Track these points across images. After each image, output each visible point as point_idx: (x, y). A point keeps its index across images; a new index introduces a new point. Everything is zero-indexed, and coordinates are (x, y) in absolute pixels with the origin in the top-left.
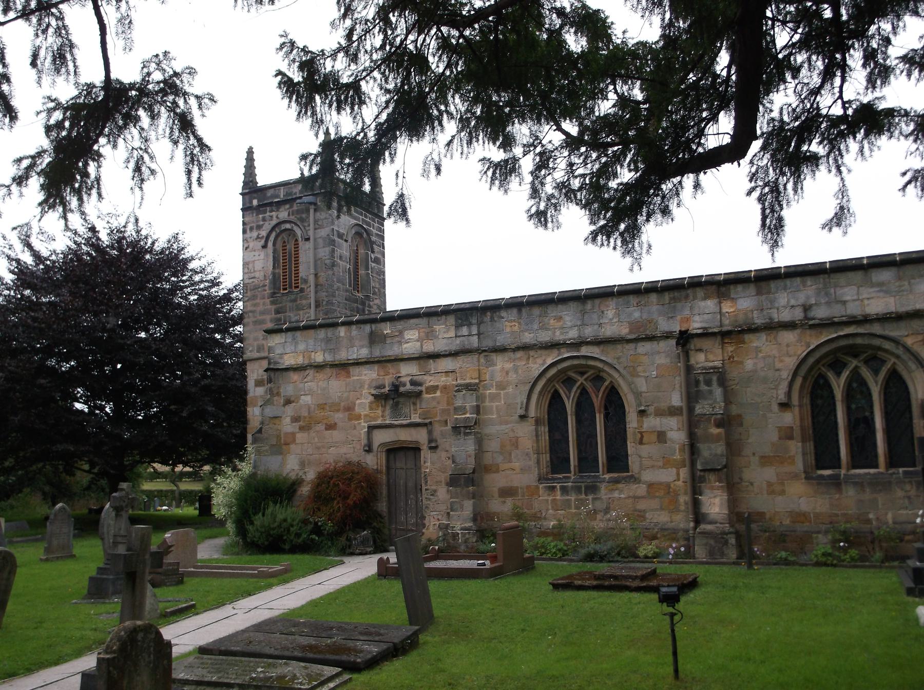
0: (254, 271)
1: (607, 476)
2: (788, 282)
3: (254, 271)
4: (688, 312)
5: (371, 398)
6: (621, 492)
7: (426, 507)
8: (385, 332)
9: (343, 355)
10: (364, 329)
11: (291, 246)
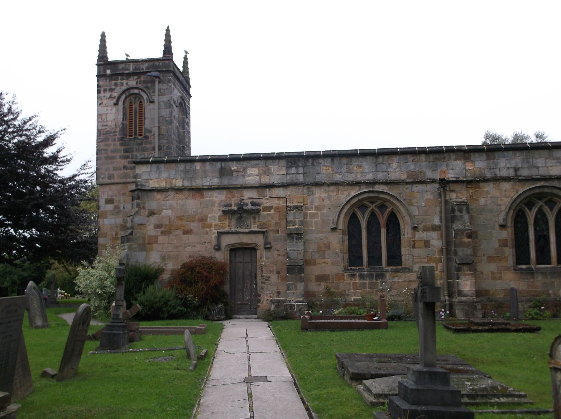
0: (107, 121)
1: (389, 268)
2: (506, 153)
3: (107, 121)
4: (445, 167)
5: (220, 213)
6: (400, 278)
7: (262, 288)
8: (232, 168)
9: (199, 182)
10: (215, 165)
11: (136, 106)
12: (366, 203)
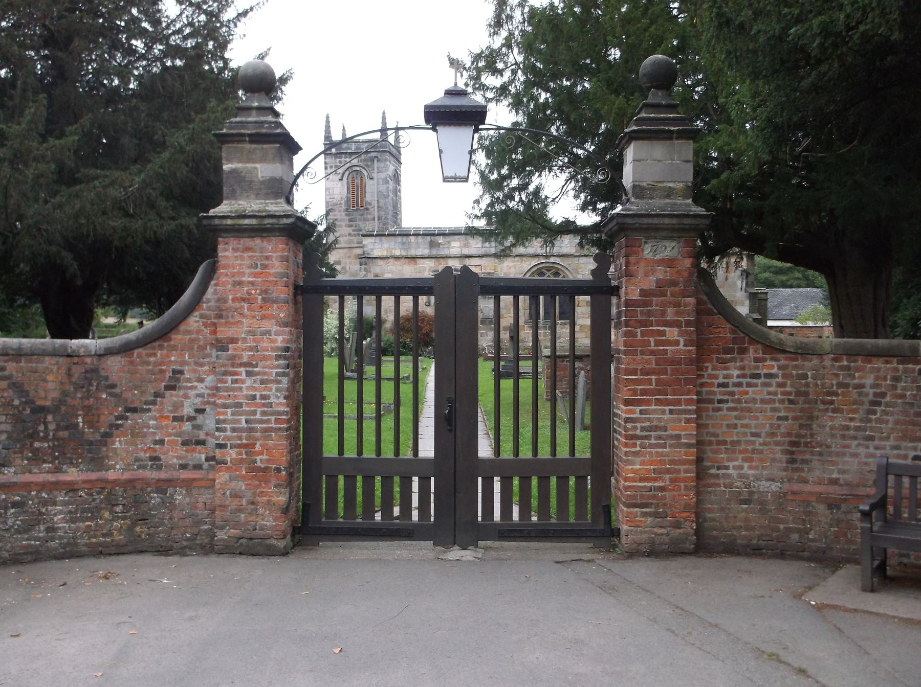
9: (413, 252)
11: (358, 181)
12: (544, 271)
